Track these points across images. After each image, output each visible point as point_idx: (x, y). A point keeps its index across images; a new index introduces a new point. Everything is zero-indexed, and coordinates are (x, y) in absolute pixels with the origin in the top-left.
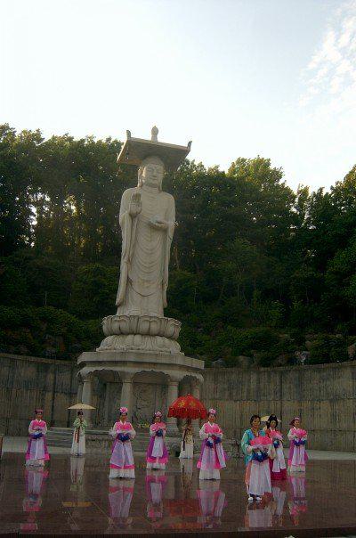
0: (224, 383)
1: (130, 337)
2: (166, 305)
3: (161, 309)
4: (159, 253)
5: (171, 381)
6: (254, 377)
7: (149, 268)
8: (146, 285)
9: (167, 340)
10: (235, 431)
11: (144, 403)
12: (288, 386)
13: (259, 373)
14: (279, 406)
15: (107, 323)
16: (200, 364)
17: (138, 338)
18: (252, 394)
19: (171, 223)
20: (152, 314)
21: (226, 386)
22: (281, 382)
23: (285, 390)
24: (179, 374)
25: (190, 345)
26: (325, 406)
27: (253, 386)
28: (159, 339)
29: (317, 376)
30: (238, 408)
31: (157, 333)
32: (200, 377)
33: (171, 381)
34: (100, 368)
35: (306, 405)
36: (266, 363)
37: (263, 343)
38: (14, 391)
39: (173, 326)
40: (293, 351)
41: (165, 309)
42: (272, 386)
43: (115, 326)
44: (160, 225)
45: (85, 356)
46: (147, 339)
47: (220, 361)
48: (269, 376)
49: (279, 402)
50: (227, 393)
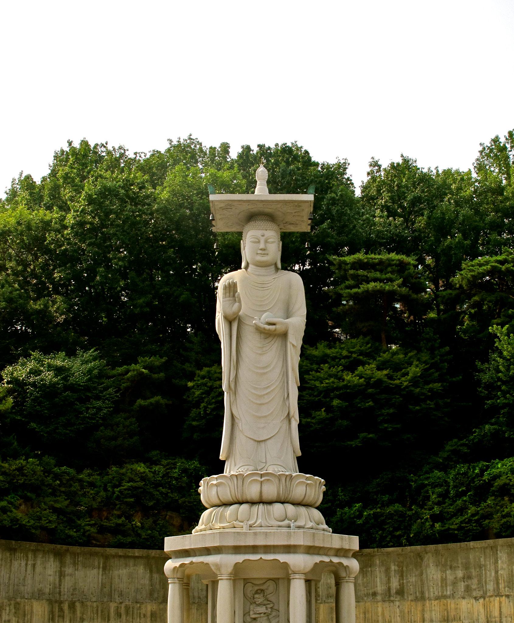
2: (299, 454)
11: (262, 609)
15: (208, 488)
16: (353, 542)
17: (245, 507)
18: (501, 586)
24: (300, 562)
28: (278, 507)
32: (354, 564)
39: (313, 487)
41: (298, 458)
45: (171, 543)
50: (462, 586)
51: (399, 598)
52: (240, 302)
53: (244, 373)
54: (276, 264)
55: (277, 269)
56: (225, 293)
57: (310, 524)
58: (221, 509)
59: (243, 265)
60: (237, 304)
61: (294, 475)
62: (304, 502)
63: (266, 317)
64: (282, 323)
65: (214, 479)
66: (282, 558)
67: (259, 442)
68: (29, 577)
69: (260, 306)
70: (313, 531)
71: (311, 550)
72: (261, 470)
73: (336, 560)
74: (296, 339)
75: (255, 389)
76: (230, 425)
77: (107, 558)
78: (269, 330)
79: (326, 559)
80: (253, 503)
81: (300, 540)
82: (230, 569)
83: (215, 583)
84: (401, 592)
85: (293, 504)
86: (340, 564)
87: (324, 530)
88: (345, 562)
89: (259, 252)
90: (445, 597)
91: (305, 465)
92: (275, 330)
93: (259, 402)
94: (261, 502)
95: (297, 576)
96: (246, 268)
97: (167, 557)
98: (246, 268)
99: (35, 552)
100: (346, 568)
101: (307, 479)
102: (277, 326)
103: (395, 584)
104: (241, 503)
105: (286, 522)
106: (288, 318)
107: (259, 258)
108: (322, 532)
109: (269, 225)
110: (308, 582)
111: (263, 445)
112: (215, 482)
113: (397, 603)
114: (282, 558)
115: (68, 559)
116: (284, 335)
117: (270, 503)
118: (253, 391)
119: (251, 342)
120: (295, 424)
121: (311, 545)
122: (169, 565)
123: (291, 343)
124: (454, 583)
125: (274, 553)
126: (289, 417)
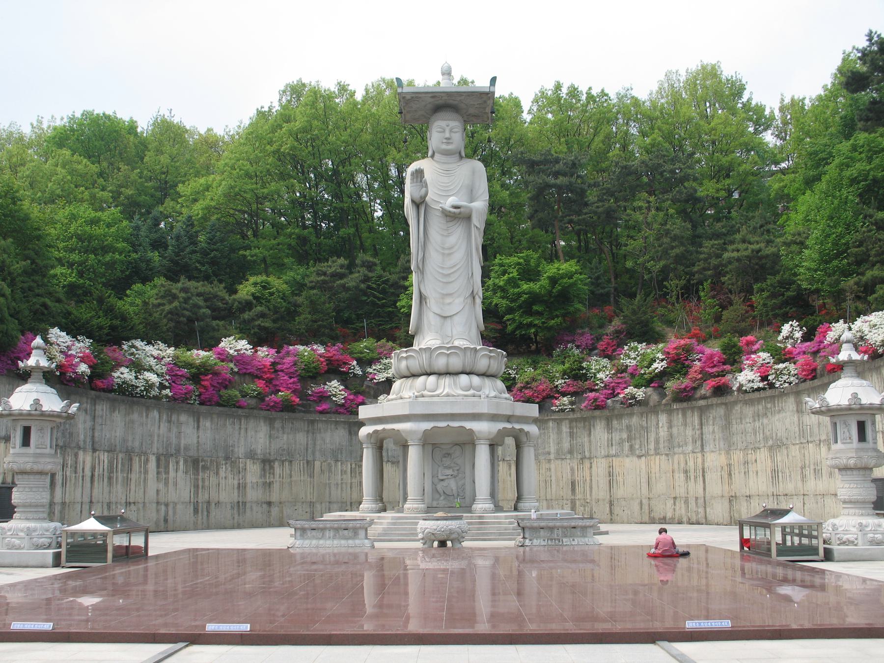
0: (621, 430)
1: (422, 378)
2: (482, 327)
3: (475, 334)
4: (459, 255)
6: (663, 418)
8: (448, 300)
9: (476, 380)
10: (641, 503)
11: (450, 472)
12: (711, 428)
13: (670, 412)
14: (700, 460)
15: (399, 360)
16: (533, 410)
17: (432, 379)
18: (661, 446)
19: (480, 205)
20: (456, 343)
21: (625, 436)
22: (701, 424)
23: (707, 437)
26: (763, 455)
27: (663, 433)
28: (464, 378)
29: (749, 411)
30: (643, 467)
31: (460, 370)
32: (533, 429)
34: (379, 427)
35: (737, 456)
38: (317, 464)
39: (494, 359)
42: (689, 432)
45: (364, 412)
46: (447, 381)
48: (684, 415)
49: (699, 455)
50: (626, 445)
51: (569, 456)
52: (426, 186)
54: (460, 153)
55: (461, 157)
56: (412, 179)
57: (493, 394)
58: (410, 380)
59: (430, 153)
60: (424, 189)
62: (488, 373)
63: (452, 200)
64: (466, 207)
65: (403, 352)
66: (469, 425)
67: (445, 318)
68: (242, 439)
70: (497, 400)
71: (494, 418)
72: (447, 343)
73: (517, 426)
74: (479, 222)
75: (443, 268)
76: (418, 302)
77: (312, 422)
78: (454, 213)
79: (509, 426)
80: (440, 374)
82: (420, 436)
83: (405, 447)
84: (571, 452)
85: (478, 375)
86: (521, 430)
87: (506, 399)
88: (526, 428)
89: (445, 141)
92: (460, 213)
95: (482, 442)
96: (432, 156)
97: (362, 424)
98: (432, 156)
99: (247, 417)
100: (527, 434)
101: (491, 351)
102: (462, 210)
103: (566, 445)
104: (429, 374)
105: (472, 392)
106: (471, 202)
107: (444, 147)
108: (505, 401)
109: (454, 115)
110: (490, 445)
111: (449, 320)
112: (404, 355)
113: (568, 461)
114: (469, 425)
115: (278, 424)
116: (468, 218)
117: (457, 374)
118: (441, 271)
119: (436, 225)
120: (479, 301)
121: (495, 412)
122: (364, 431)
123: (475, 226)
125: (460, 420)
126: (473, 296)
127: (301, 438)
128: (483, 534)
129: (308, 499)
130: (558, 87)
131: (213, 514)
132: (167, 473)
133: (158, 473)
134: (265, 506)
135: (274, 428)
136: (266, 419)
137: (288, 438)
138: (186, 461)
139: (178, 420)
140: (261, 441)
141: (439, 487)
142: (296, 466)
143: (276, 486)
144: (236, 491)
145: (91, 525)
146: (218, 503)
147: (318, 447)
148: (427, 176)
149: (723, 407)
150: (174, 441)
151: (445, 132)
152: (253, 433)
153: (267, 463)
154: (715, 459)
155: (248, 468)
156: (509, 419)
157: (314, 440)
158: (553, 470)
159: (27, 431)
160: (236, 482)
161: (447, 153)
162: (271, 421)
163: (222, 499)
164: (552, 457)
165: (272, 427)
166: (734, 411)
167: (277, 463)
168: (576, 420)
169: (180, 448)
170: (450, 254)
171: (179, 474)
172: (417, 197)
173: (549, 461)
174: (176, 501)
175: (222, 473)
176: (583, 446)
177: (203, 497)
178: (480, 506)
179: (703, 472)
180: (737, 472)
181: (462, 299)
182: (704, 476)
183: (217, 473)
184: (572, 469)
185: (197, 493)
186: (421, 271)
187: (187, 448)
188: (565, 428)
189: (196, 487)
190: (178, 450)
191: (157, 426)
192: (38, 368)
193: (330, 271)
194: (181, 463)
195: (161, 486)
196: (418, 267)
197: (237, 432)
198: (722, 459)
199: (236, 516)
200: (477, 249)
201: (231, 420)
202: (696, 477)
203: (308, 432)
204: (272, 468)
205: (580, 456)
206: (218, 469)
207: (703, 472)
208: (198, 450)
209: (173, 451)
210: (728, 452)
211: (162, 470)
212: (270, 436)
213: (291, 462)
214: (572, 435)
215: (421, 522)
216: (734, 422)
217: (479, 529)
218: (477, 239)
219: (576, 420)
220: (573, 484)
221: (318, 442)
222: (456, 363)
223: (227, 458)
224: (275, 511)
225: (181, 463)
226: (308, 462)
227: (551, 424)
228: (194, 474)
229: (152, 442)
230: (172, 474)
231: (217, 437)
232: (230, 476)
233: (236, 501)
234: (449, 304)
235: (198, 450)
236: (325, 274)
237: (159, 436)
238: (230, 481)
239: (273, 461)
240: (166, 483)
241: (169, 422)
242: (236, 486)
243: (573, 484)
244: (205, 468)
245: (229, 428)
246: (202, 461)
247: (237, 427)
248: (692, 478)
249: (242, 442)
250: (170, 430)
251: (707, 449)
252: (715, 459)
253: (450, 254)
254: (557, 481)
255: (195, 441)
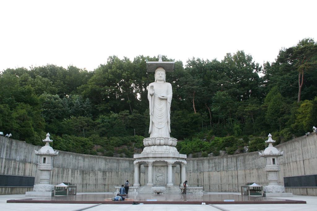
0: (212, 163)
2: (170, 132)
4: (164, 110)
5: (169, 164)
6: (225, 160)
7: (160, 116)
8: (160, 124)
11: (160, 174)
12: (239, 163)
13: (227, 158)
14: (236, 173)
15: (146, 141)
16: (185, 156)
18: (225, 168)
19: (170, 96)
21: (214, 165)
22: (236, 162)
23: (239, 165)
24: (171, 161)
25: (180, 148)
26: (255, 171)
27: (225, 164)
28: (165, 146)
29: (251, 157)
32: (185, 162)
33: (169, 164)
35: (248, 171)
36: (231, 153)
37: (228, 144)
38: (120, 173)
39: (174, 141)
40: (243, 146)
42: (233, 164)
43: (150, 143)
44: (163, 98)
46: (160, 147)
47: (212, 153)
48: (231, 159)
49: (236, 171)
50: (214, 168)
53: (155, 110)
55: (164, 82)
57: (173, 151)
59: (155, 81)
61: (169, 138)
65: (147, 139)
68: (97, 165)
69: (160, 92)
73: (180, 161)
75: (159, 114)
76: (151, 124)
79: (178, 161)
81: (171, 156)
83: (147, 167)
84: (197, 170)
90: (210, 171)
91: (172, 135)
93: (160, 118)
94: (160, 145)
99: (99, 158)
102: (165, 97)
103: (196, 168)
104: (154, 145)
106: (167, 95)
110: (172, 167)
112: (147, 140)
115: (108, 160)
116: (166, 99)
117: (163, 145)
118: (159, 115)
119: (157, 102)
120: (169, 124)
122: (135, 162)
124: (212, 167)
127: (115, 165)
128: (170, 192)
129: (117, 184)
130: (194, 58)
131: (87, 188)
132: (74, 175)
133: (72, 175)
134: (103, 185)
135: (107, 161)
136: (104, 158)
137: (111, 165)
138: (80, 171)
139: (78, 158)
140: (103, 165)
141: (157, 179)
142: (113, 174)
143: (107, 180)
144: (95, 181)
145: (63, 185)
146: (89, 184)
147: (120, 168)
148: (155, 88)
149: (243, 156)
150: (77, 165)
151: (160, 74)
152: (100, 163)
153: (104, 172)
154: (241, 172)
155: (99, 173)
156: (178, 158)
157: (119, 165)
158: (192, 175)
159: (45, 159)
160: (95, 178)
161: (160, 81)
162: (106, 159)
163: (90, 183)
164: (191, 171)
165: (106, 161)
166: (246, 158)
167: (107, 172)
168: (199, 160)
169: (78, 167)
170: (161, 110)
171: (78, 175)
172: (152, 93)
173: (191, 173)
174: (77, 183)
175: (91, 175)
176: (201, 168)
177: (85, 182)
178: (170, 184)
179: (237, 176)
180: (247, 176)
181: (164, 124)
182: (238, 178)
183: (89, 175)
184: (198, 176)
185: (83, 181)
186: (152, 115)
187: (80, 167)
188: (195, 163)
189: (83, 179)
190: (78, 168)
191: (72, 160)
192: (48, 142)
193: (124, 114)
194: (79, 172)
195: (73, 179)
196: (152, 114)
197: (95, 163)
198: (243, 172)
199: (95, 189)
200: (169, 109)
201: (94, 159)
202: (235, 178)
203: (117, 163)
204: (106, 174)
205: (200, 171)
206: (89, 174)
207: (237, 176)
208: (84, 168)
209: (76, 168)
210: (245, 170)
211: (73, 174)
212: (106, 164)
213: (112, 172)
214: (197, 165)
215: (153, 187)
216: (246, 161)
217: (169, 191)
218: (169, 106)
219: (199, 160)
220: (198, 180)
221: (120, 166)
222: (162, 142)
223: (92, 170)
224: (106, 187)
225: (79, 172)
226: (117, 172)
227: (191, 161)
228: (82, 175)
229: (70, 165)
230: (76, 175)
231: (89, 164)
232: (93, 176)
233: (95, 184)
234: (161, 125)
235: (84, 168)
236: (123, 115)
237: (72, 163)
238: (93, 177)
239: (106, 172)
240: (74, 178)
241: (76, 159)
242: (95, 179)
243: (198, 180)
244: (86, 173)
245: (93, 161)
246: (85, 171)
247: (96, 161)
248: (234, 178)
249: (97, 166)
250: (76, 162)
251: (238, 169)
252: (241, 172)
253: (161, 110)
254: (193, 179)
255: (83, 165)
